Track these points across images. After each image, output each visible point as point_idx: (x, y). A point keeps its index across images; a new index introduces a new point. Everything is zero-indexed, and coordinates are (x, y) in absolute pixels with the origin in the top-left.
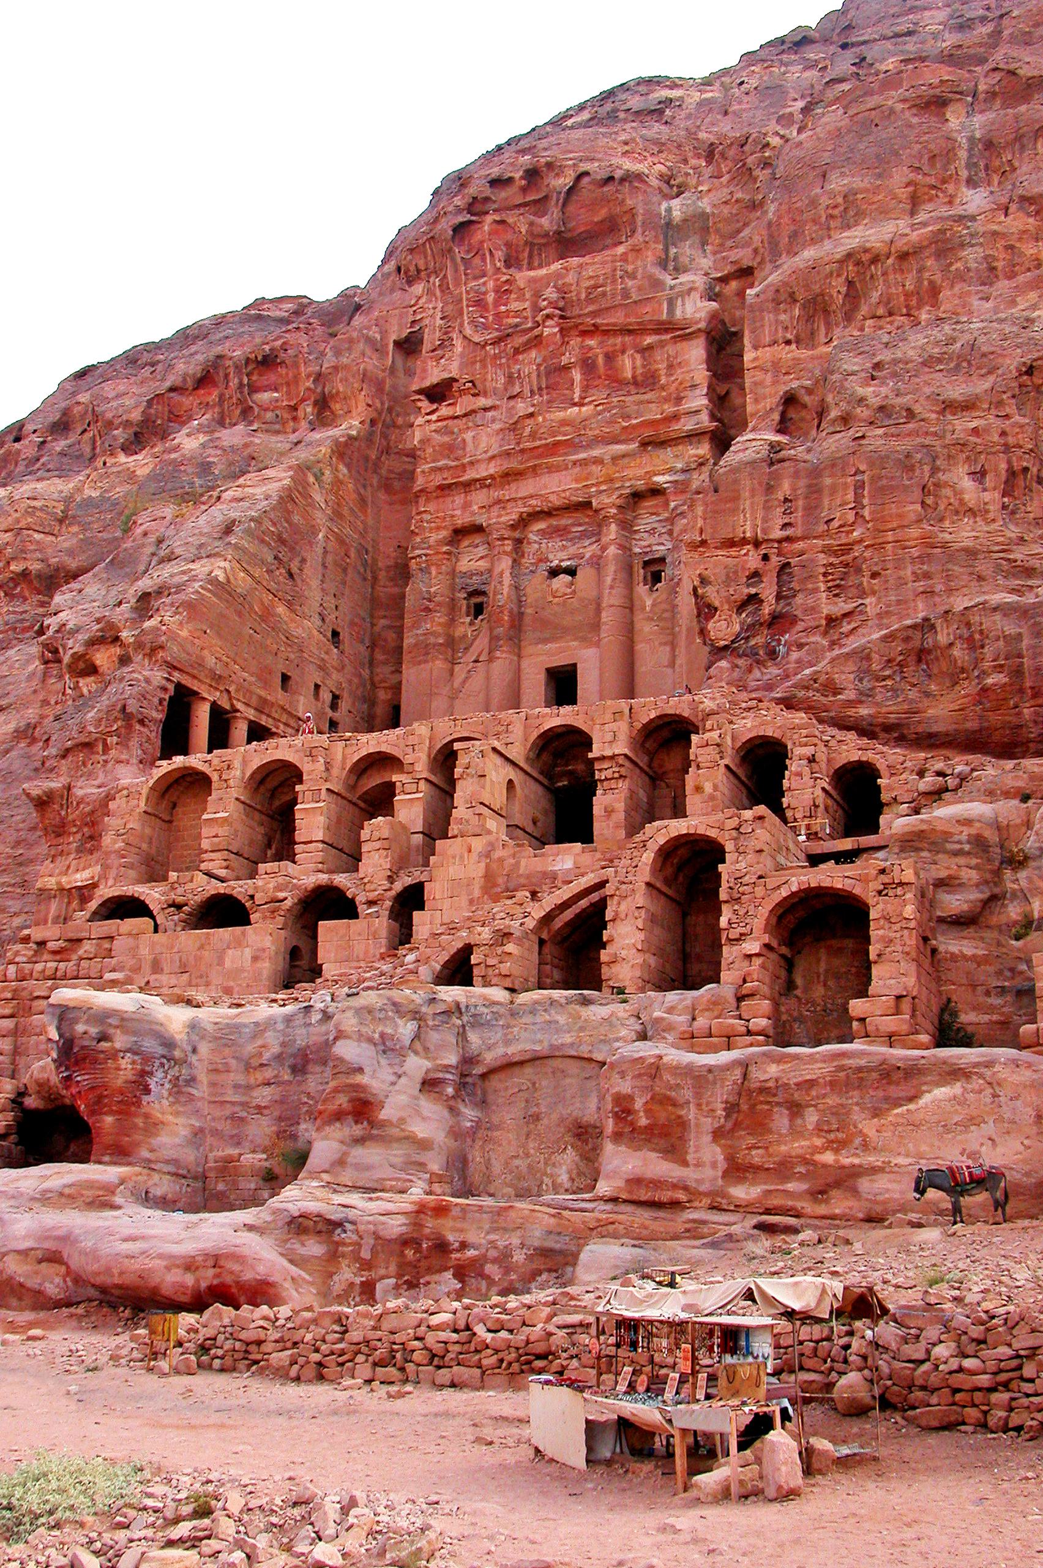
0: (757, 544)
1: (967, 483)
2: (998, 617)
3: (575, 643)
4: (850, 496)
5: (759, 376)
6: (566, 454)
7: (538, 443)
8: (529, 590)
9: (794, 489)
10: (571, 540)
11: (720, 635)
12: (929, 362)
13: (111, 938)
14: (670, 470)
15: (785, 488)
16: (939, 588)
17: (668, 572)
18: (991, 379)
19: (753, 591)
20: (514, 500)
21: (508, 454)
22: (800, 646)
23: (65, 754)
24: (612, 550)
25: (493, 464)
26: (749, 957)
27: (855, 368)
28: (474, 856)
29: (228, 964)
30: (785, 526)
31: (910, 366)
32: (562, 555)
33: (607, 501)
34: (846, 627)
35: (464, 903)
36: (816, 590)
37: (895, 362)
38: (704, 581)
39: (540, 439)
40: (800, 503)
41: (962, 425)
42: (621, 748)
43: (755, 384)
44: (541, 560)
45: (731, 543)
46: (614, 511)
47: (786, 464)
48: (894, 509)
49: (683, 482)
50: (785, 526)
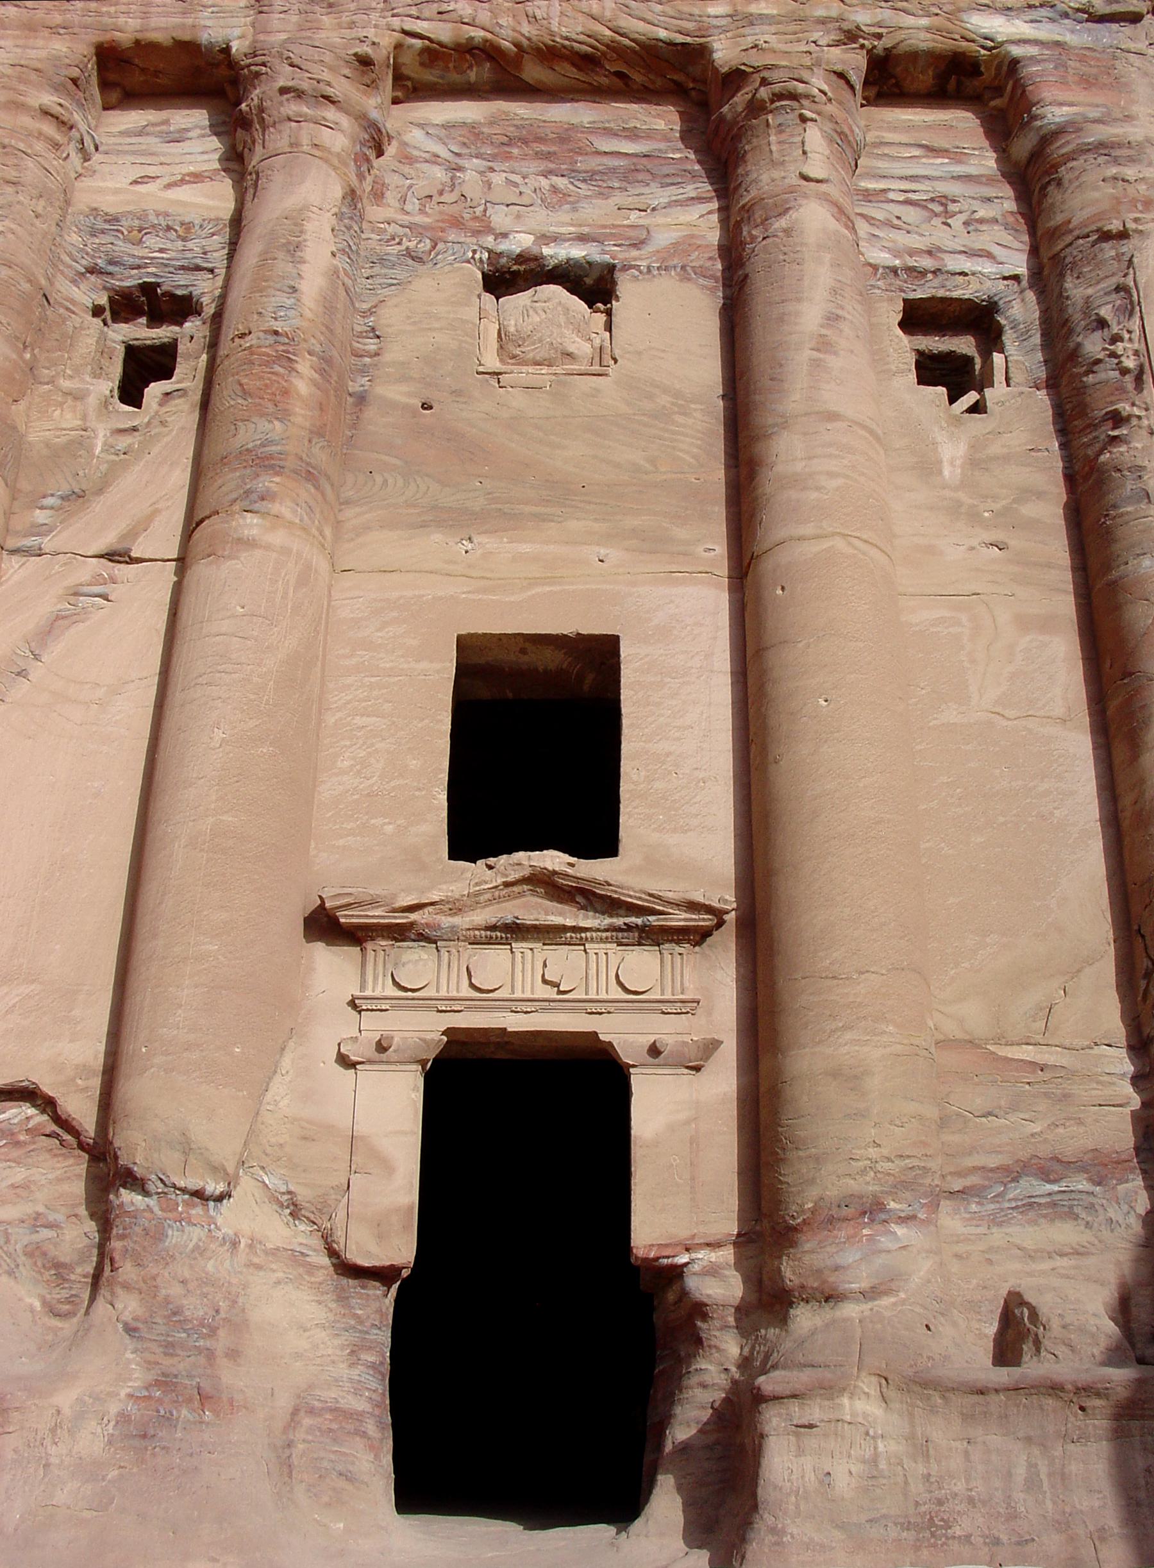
3: (614, 554)
8: (391, 317)
10: (590, 177)
17: (1019, 358)
24: (813, 218)
32: (560, 221)
44: (457, 223)
46: (818, 82)
49: (1084, 55)
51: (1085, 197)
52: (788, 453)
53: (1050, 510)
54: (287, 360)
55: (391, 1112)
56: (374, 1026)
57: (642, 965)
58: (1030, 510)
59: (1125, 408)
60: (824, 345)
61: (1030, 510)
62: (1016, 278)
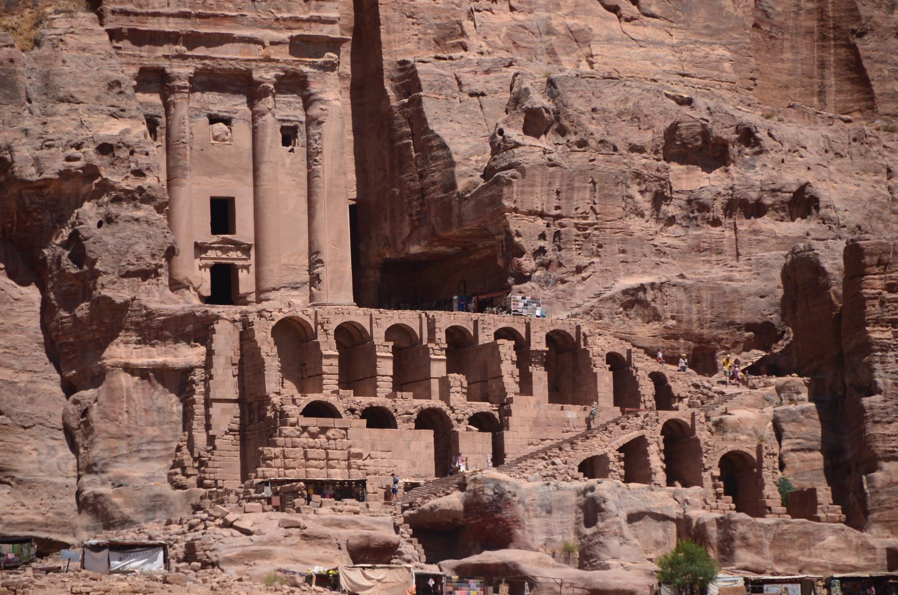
0: (542, 215)
1: (638, 197)
2: (674, 289)
3: (234, 182)
4: (588, 194)
5: (390, 13)
6: (231, 28)
7: (209, 12)
8: (194, 131)
9: (561, 185)
11: (528, 269)
12: (620, 114)
13: (346, 429)
14: (313, 65)
15: (556, 186)
16: (630, 260)
17: (301, 139)
18: (650, 132)
19: (542, 243)
20: (193, 57)
21: (185, 15)
22: (563, 282)
23: (128, 275)
25: (171, 20)
26: (713, 478)
27: (582, 109)
28: (532, 406)
29: (412, 448)
30: (557, 208)
31: (611, 115)
33: (266, 75)
34: (584, 274)
35: (527, 428)
36: (570, 249)
37: (604, 111)
38: (519, 235)
39: (211, 9)
40: (563, 195)
41: (639, 160)
42: (543, 347)
43: (387, 18)
45: (530, 213)
46: (272, 86)
47: (558, 169)
48: (610, 209)
50: (557, 208)
51: (315, 111)
52: (266, 170)
53: (304, 174)
54: (185, 148)
55: (207, 275)
56: (204, 262)
57: (239, 253)
58: (300, 173)
59: (317, 158)
60: (271, 147)
61: (300, 173)
62: (301, 122)
